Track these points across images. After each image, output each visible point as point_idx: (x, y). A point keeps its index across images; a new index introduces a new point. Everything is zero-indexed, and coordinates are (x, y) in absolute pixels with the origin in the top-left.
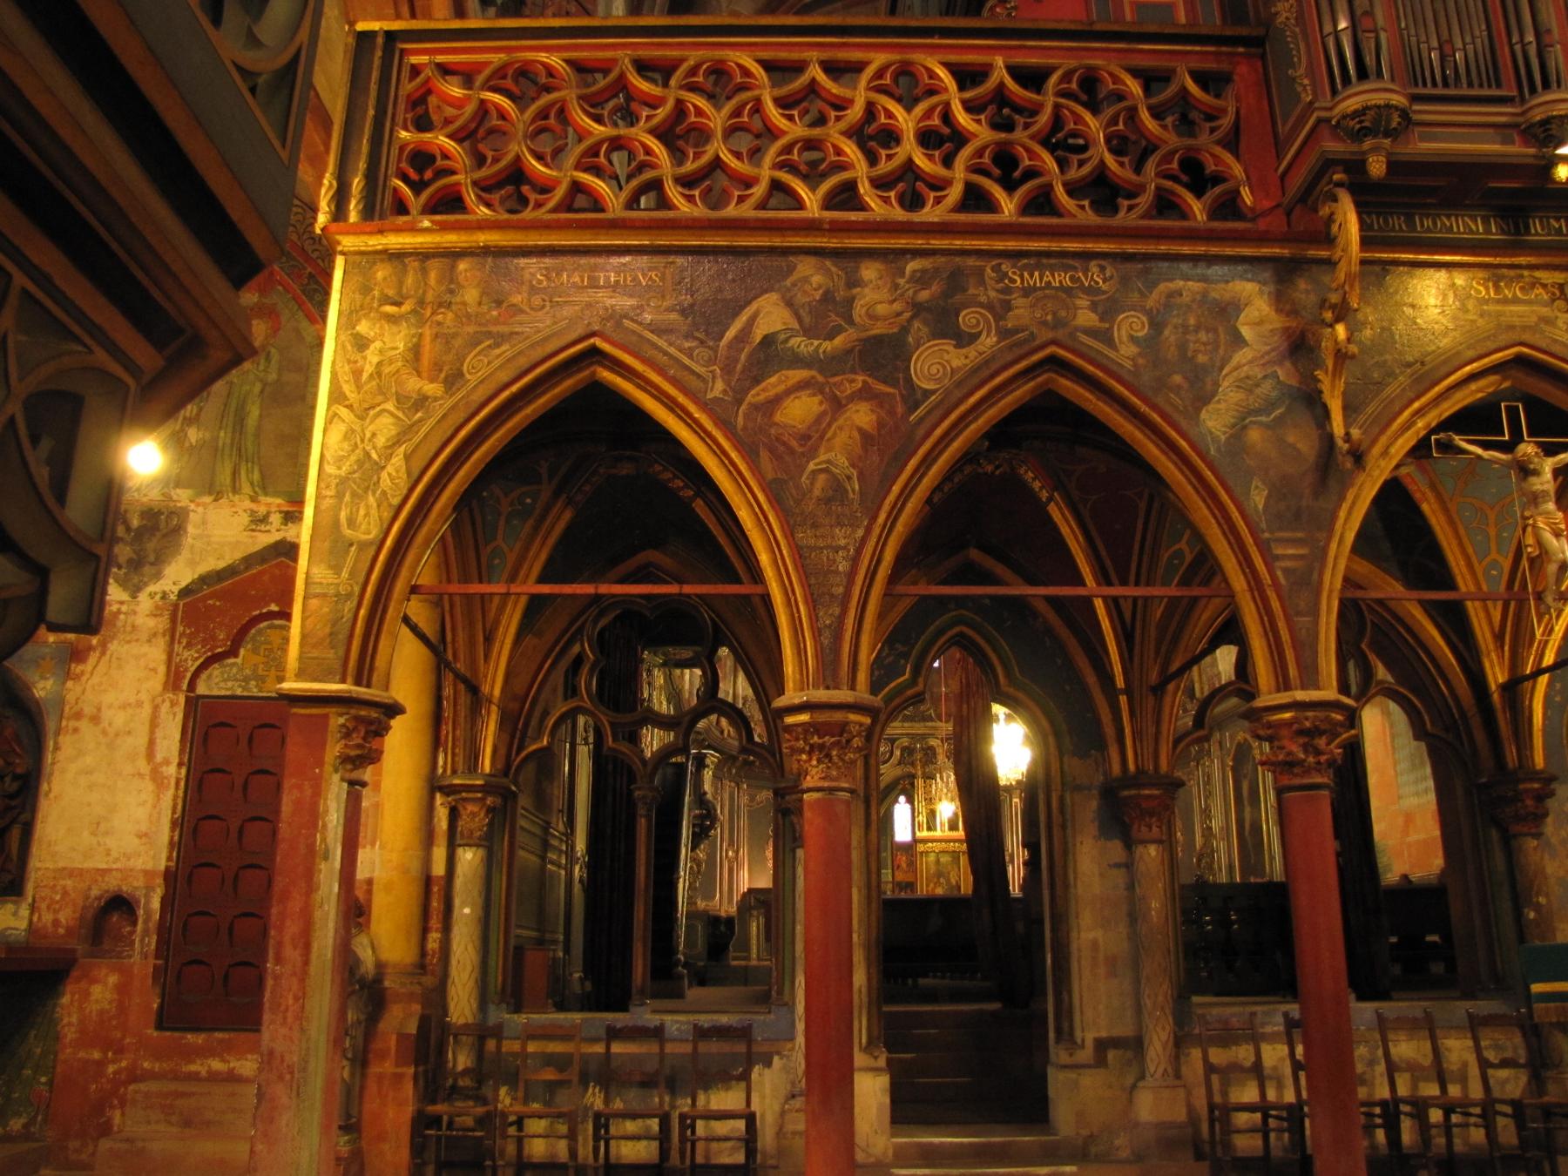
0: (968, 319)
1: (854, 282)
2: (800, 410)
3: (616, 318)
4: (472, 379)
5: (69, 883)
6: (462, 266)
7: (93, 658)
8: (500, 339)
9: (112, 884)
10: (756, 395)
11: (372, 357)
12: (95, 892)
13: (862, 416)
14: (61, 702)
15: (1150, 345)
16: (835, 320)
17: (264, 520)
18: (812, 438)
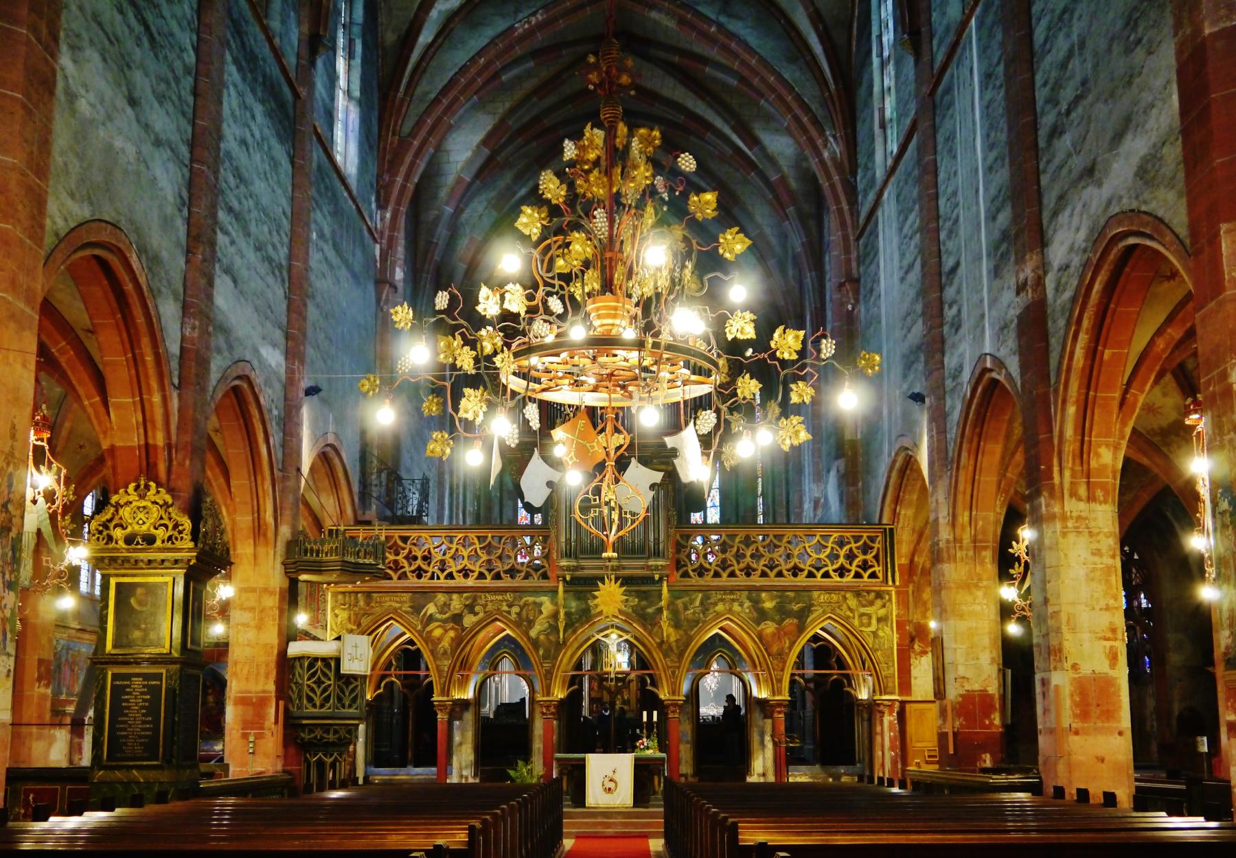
0: (477, 609)
1: (451, 600)
2: (437, 633)
3: (395, 611)
4: (363, 625)
6: (359, 595)
8: (369, 615)
10: (428, 629)
11: (339, 619)
13: (452, 634)
15: (519, 614)
16: (446, 609)
18: (440, 639)
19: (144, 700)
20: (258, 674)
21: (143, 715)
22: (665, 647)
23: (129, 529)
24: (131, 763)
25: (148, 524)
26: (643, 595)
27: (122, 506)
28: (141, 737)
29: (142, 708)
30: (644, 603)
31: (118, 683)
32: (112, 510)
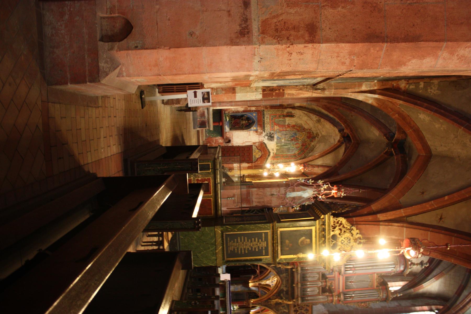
5: (231, 135)
7: (256, 133)
9: (232, 140)
12: (231, 138)
14: (251, 131)
17: (273, 150)
19: (255, 248)
20: (260, 198)
21: (248, 249)
22: (269, 301)
23: (339, 236)
24: (225, 246)
25: (341, 245)
26: (287, 292)
27: (350, 232)
28: (238, 249)
29: (252, 248)
30: (284, 293)
31: (263, 235)
32: (349, 227)
